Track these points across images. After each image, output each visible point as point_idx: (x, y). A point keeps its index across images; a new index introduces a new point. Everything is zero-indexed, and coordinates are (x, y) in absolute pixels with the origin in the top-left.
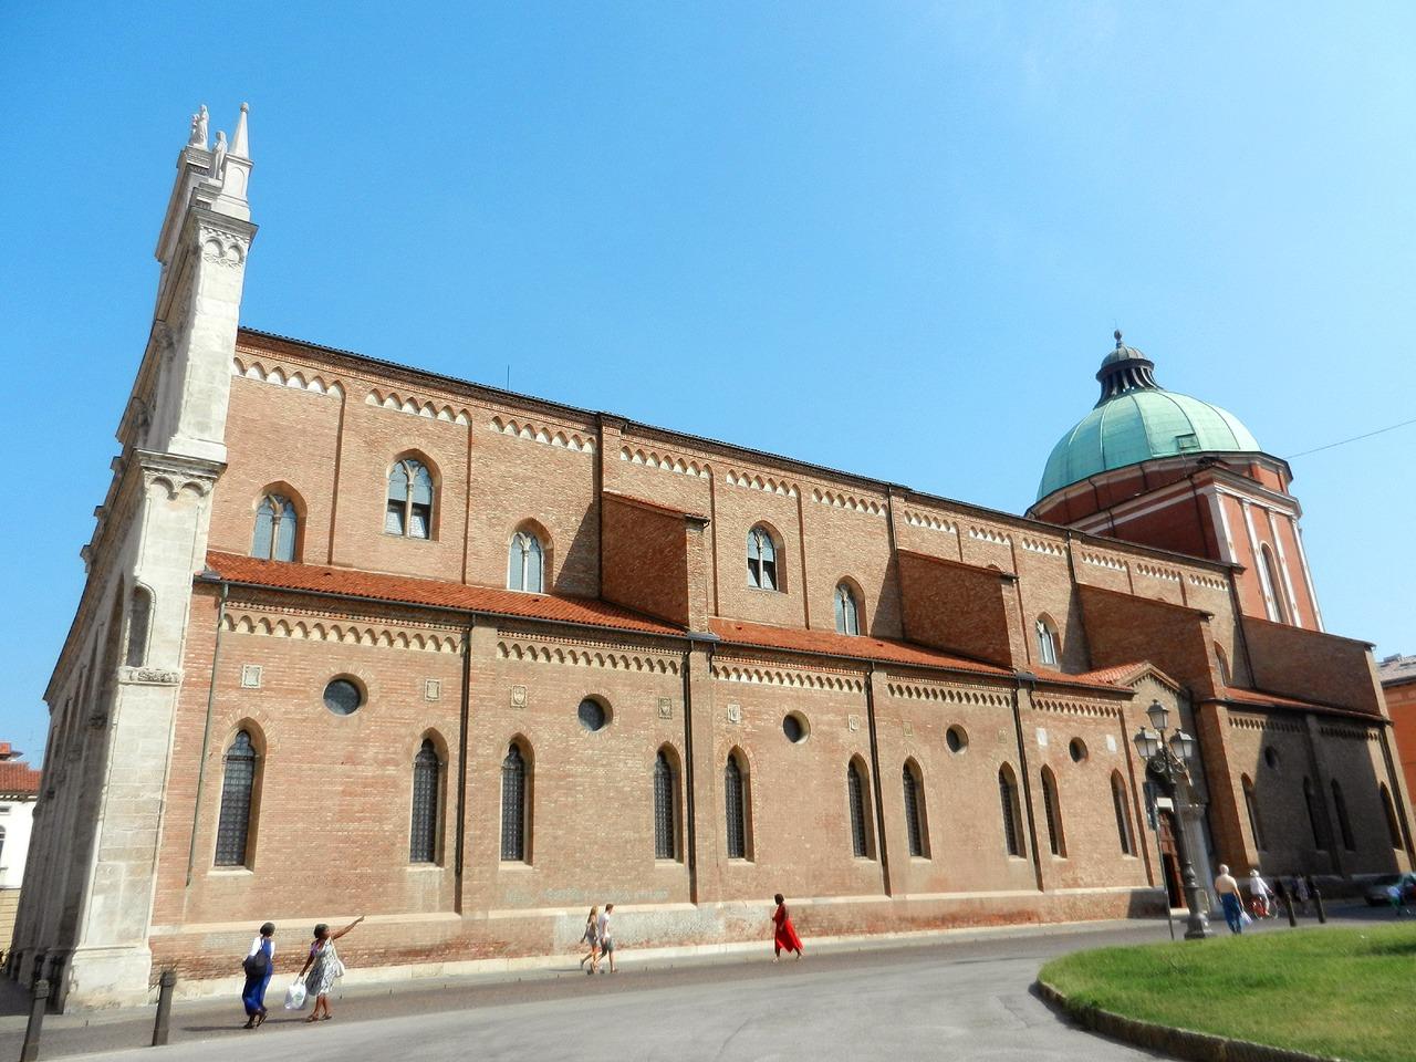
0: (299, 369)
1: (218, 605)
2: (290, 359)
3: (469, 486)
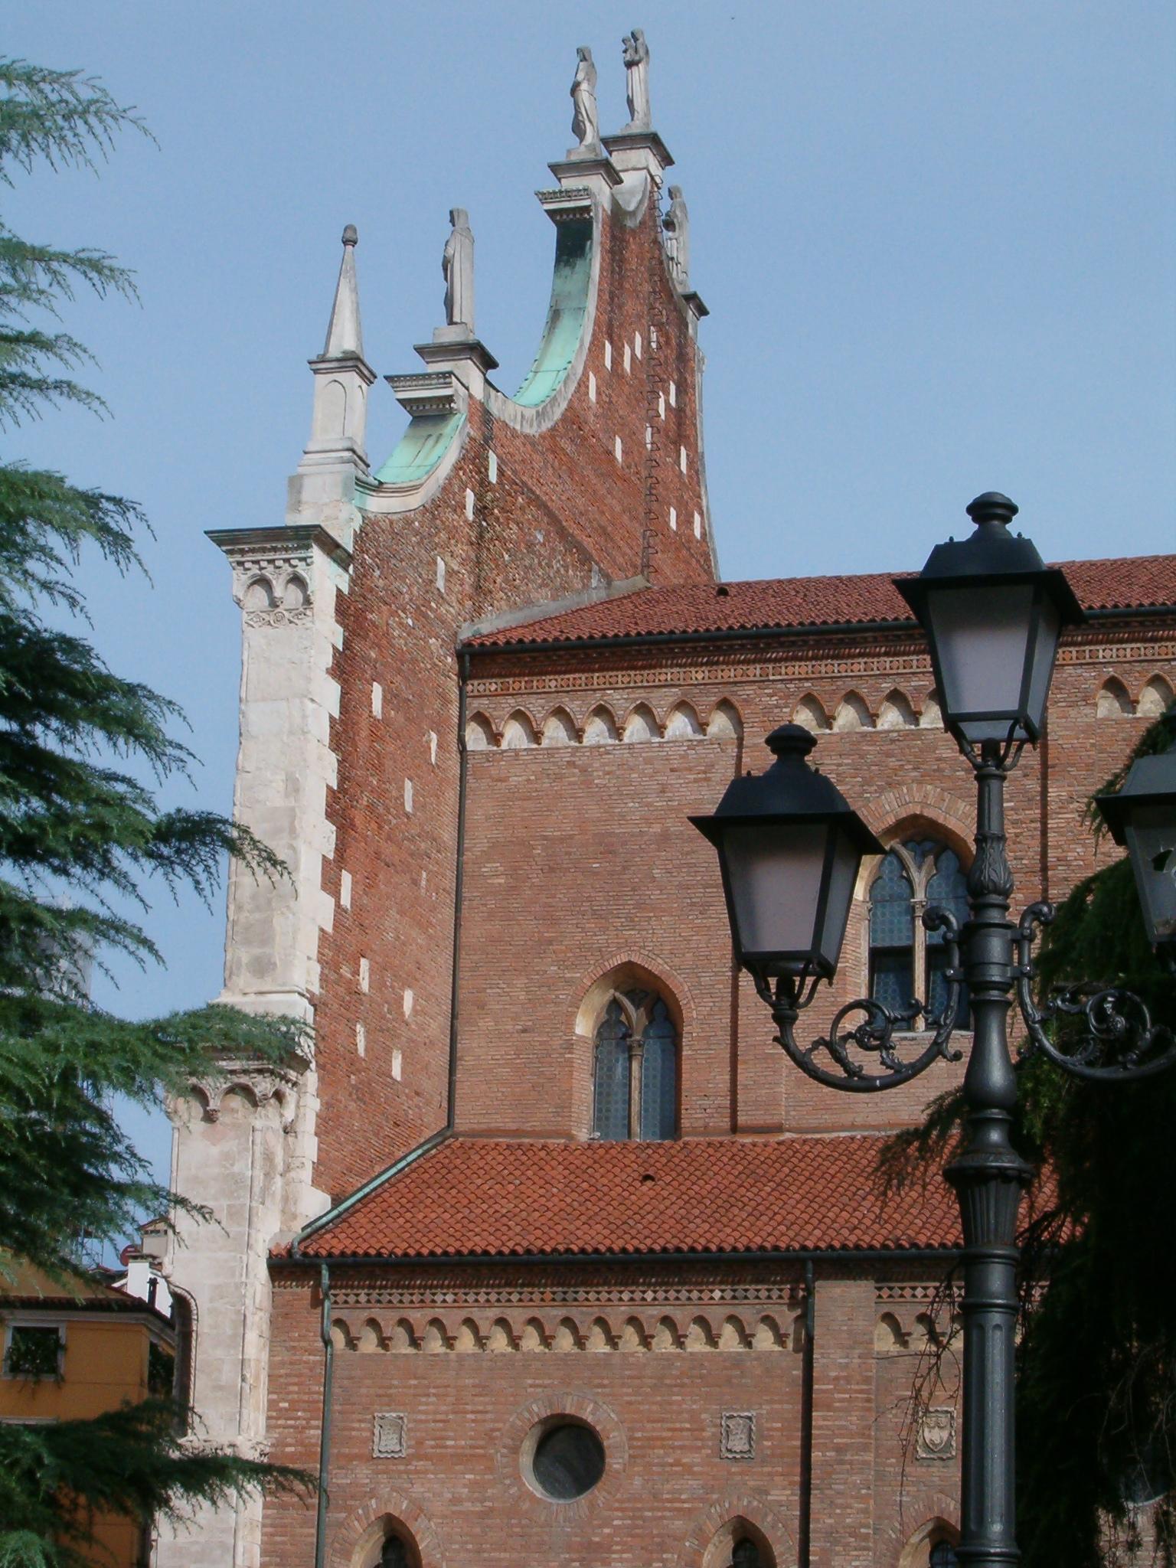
0: (640, 695)
1: (317, 1302)
2: (621, 677)
3: (1045, 879)
